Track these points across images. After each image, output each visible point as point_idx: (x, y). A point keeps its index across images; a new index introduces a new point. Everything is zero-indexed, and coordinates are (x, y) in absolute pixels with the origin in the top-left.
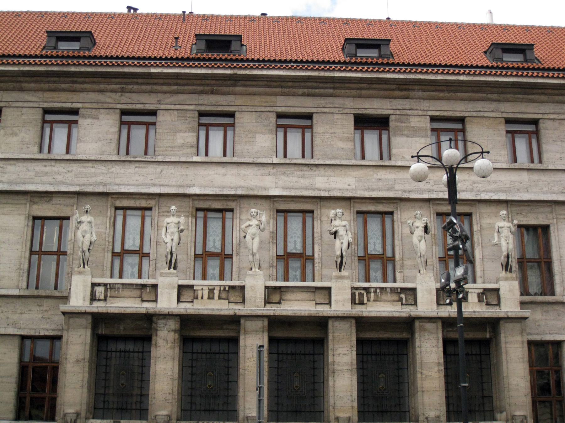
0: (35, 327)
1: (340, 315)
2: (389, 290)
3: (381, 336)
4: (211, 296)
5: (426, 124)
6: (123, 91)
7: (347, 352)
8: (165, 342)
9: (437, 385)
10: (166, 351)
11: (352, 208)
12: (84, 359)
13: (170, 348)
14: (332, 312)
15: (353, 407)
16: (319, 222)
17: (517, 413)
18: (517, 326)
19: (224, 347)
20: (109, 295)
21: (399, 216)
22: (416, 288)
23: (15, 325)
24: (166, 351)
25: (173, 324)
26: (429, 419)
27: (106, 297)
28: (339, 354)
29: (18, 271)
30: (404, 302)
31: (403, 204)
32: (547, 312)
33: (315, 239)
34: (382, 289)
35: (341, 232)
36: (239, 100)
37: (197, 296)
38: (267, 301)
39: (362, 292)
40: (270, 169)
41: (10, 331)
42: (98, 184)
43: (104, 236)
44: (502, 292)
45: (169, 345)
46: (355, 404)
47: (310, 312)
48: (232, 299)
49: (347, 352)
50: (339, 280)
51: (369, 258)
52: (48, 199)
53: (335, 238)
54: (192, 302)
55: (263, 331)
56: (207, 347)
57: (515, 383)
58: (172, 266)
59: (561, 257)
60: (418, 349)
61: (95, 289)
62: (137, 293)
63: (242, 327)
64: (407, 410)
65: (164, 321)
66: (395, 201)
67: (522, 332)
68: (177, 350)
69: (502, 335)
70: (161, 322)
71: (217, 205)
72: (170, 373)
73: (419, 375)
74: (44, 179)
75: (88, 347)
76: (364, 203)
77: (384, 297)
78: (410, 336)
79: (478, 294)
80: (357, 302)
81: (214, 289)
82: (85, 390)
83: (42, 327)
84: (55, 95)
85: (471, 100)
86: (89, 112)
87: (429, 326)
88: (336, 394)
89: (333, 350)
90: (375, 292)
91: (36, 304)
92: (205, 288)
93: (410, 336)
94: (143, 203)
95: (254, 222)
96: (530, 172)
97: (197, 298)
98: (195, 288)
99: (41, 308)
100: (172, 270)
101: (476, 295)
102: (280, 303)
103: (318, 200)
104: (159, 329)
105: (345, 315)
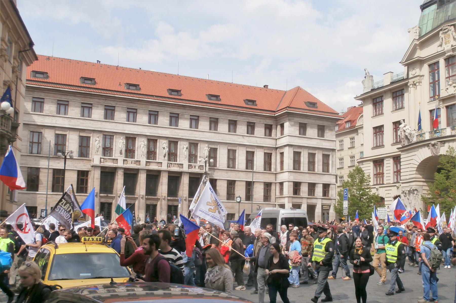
5: (189, 117)
6: (106, 100)
23: (76, 167)
36: (139, 106)
38: (146, 165)
40: (146, 127)
42: (99, 128)
68: (123, 177)
71: (132, 136)
84: (86, 99)
85: (201, 111)
86: (95, 105)
94: (111, 134)
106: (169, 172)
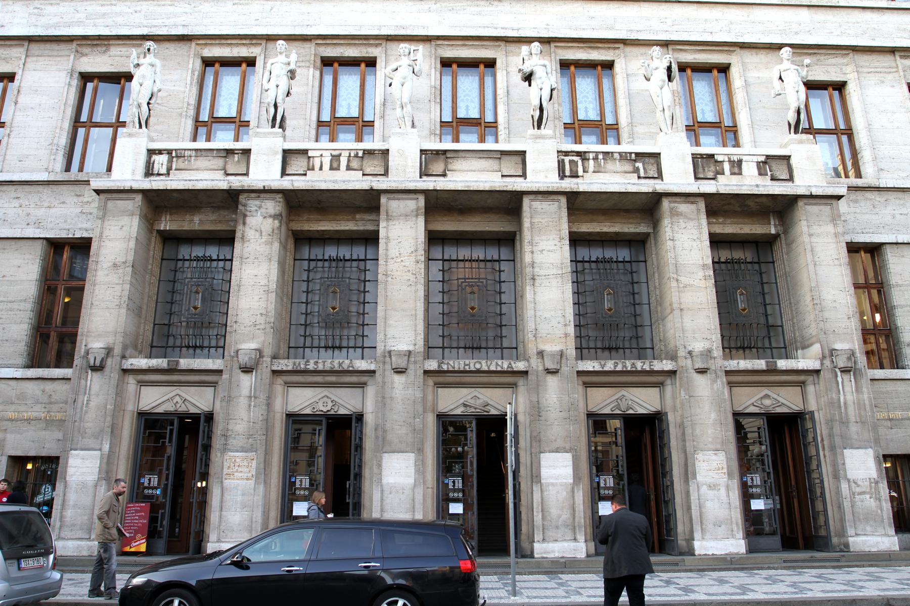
0: (67, 227)
1: (541, 190)
2: (616, 156)
3: (605, 229)
4: (335, 165)
7: (555, 248)
8: (258, 234)
9: (704, 300)
10: (258, 248)
11: (553, 55)
12: (125, 263)
13: (267, 243)
14: (529, 185)
15: (566, 335)
16: (505, 72)
17: (838, 346)
18: (825, 210)
19: (358, 251)
20: (174, 167)
21: (624, 66)
22: (659, 154)
23: (38, 224)
24: (258, 248)
25: (272, 206)
26: (694, 354)
27: (169, 169)
28: (542, 251)
29: (50, 147)
30: (642, 174)
31: (629, 49)
32: (856, 201)
33: (498, 98)
34: (606, 154)
35: (539, 73)
37: (313, 166)
39: (576, 158)
41: (30, 232)
43: (182, 96)
44: (793, 161)
45: (265, 238)
46: (571, 330)
47: (493, 184)
48: (368, 171)
49: (555, 248)
50: (538, 141)
51: (580, 126)
52: (104, 49)
53: (530, 85)
54: (305, 175)
55: (417, 216)
56: (331, 251)
57: (830, 297)
58: (277, 125)
59: (870, 125)
60: (669, 244)
61: (152, 159)
62: (220, 162)
63: (382, 209)
64: (649, 345)
65: (257, 202)
66: (616, 46)
67: (835, 218)
68: (276, 246)
69: (803, 223)
70: (253, 204)
72: (264, 282)
73: (674, 284)
74: (99, 21)
75: (132, 244)
76: (569, 47)
77: (610, 166)
78: (650, 230)
79: (758, 163)
80: (568, 173)
81: (340, 155)
82: (124, 311)
83: (80, 226)
87: (684, 207)
88: (538, 314)
89: (531, 243)
90: (596, 159)
91: (73, 194)
92: (325, 153)
93: (650, 230)
94: (242, 52)
95: (405, 61)
96: (813, 10)
97: (313, 169)
98: (310, 154)
99: (81, 199)
100: (277, 130)
101: (755, 164)
102: (444, 175)
103: (502, 44)
104: (248, 213)
105: (550, 190)
106: (577, 204)
